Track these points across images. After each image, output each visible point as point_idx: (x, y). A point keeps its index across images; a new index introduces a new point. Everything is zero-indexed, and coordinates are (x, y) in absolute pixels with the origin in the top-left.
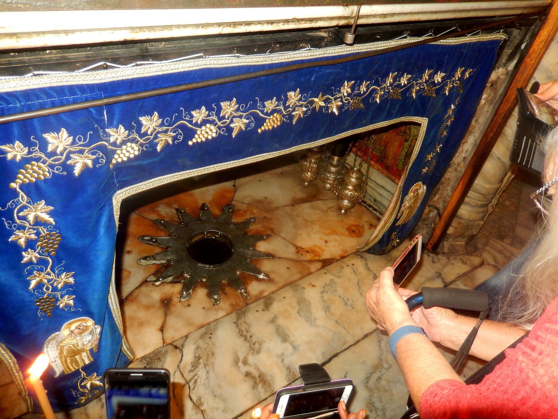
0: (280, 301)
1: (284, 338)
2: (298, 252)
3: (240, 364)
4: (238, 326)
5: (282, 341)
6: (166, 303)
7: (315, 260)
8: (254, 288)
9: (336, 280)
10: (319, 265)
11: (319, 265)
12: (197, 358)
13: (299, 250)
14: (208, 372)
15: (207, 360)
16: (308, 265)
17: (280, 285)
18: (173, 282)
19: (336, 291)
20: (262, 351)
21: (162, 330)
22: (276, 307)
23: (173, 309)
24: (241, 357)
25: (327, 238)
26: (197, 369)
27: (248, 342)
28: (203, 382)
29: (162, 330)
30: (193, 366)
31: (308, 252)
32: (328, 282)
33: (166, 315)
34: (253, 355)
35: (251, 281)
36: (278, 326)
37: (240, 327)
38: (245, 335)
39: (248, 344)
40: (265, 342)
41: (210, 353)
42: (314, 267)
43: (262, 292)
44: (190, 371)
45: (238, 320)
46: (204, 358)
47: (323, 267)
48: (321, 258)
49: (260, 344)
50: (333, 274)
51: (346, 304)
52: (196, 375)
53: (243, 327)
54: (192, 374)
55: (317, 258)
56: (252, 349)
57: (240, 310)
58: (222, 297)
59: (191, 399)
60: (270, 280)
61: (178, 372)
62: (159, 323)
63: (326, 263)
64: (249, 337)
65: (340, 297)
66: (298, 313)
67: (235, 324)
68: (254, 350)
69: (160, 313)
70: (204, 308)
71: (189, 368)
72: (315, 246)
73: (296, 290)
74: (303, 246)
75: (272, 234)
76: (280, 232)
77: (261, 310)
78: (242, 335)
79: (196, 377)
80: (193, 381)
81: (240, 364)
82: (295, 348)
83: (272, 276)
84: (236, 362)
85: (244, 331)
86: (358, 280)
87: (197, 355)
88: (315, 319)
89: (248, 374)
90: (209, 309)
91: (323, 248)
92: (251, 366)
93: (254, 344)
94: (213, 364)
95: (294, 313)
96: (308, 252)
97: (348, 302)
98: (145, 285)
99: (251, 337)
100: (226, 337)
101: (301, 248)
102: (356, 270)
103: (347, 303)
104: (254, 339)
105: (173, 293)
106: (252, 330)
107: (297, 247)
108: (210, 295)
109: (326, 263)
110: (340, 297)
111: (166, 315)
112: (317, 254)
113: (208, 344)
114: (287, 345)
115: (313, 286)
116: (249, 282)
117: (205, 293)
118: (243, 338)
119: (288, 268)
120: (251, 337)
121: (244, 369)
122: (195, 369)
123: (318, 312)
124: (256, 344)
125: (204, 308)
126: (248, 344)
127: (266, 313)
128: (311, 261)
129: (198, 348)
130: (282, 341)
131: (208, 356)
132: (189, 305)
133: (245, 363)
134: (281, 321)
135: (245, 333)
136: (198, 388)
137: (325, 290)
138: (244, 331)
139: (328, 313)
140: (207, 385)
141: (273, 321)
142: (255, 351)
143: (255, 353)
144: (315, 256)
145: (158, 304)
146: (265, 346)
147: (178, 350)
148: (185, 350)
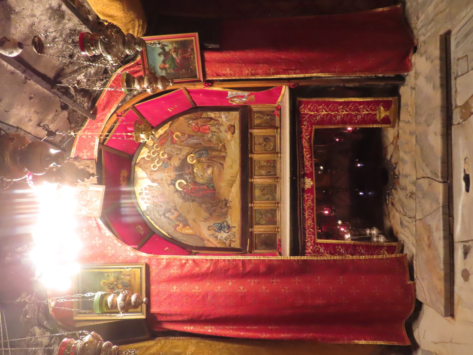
1: (406, 176)
13: (392, 143)
18: (389, 197)
23: (394, 203)
33: (394, 207)
38: (402, 189)
51: (407, 143)
62: (396, 211)
63: (398, 136)
82: (410, 175)
84: (407, 198)
89: (410, 197)
114: (409, 177)
121: (408, 197)
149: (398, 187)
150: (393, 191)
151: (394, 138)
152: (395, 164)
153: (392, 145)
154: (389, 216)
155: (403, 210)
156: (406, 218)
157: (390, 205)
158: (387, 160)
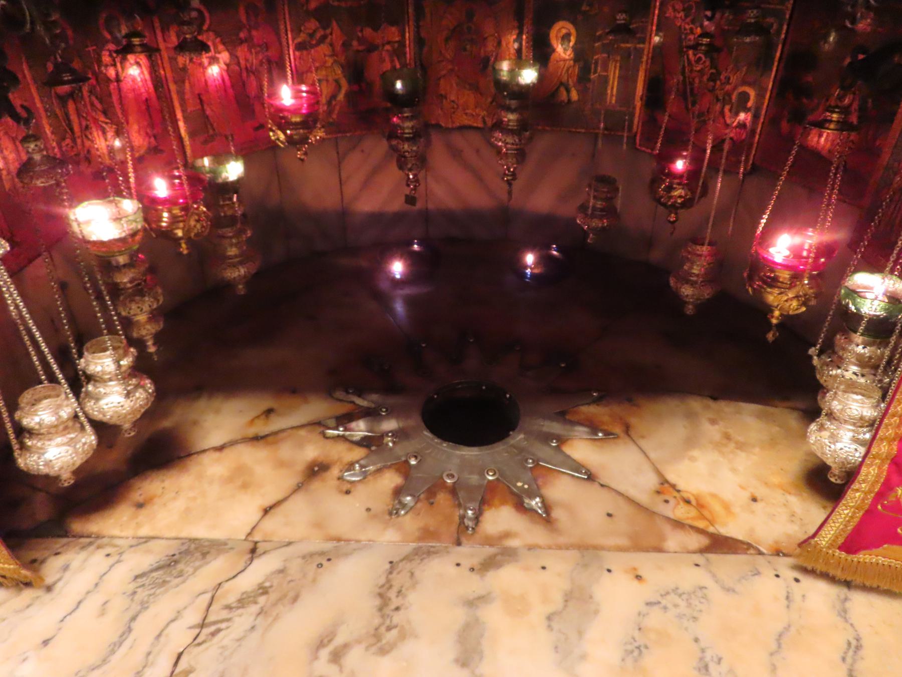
0: (526, 569)
2: (658, 492)
3: (324, 653)
4: (391, 573)
5: (457, 661)
6: (316, 470)
7: (692, 527)
8: (500, 519)
9: (715, 592)
10: (696, 541)
11: (696, 541)
12: (263, 590)
13: (665, 487)
14: (253, 628)
15: (275, 604)
16: (667, 529)
17: (562, 540)
19: (695, 619)
20: (394, 653)
21: (266, 511)
22: (508, 577)
23: (316, 485)
24: (339, 640)
25: (760, 492)
26: (240, 611)
27: (383, 616)
28: (226, 642)
29: (266, 511)
30: (240, 601)
31: (688, 502)
32: (686, 586)
33: (298, 488)
34: (367, 649)
35: (504, 502)
36: (477, 620)
37: (394, 575)
38: (386, 598)
39: (377, 621)
40: (416, 637)
41: (291, 594)
42: (674, 540)
43: (507, 535)
44: (229, 607)
45: (402, 560)
46: (273, 596)
47: (703, 551)
48: (711, 529)
49: (403, 636)
50: (714, 576)
52: (228, 620)
53: (398, 580)
54: (225, 614)
55: (701, 524)
56: (376, 635)
57: (426, 545)
58: (419, 505)
59: (176, 664)
60: (546, 518)
61: (208, 596)
63: (720, 545)
64: (393, 607)
65: (696, 640)
66: (549, 618)
67: (388, 566)
68: (379, 640)
69: (289, 480)
70: (368, 510)
71: (232, 599)
72: (714, 496)
73: (586, 566)
74: (681, 485)
75: (622, 435)
76: (643, 437)
77: (469, 566)
78: (381, 595)
79: (223, 625)
80: (213, 628)
81: (324, 653)
83: (556, 513)
84: (321, 644)
85: (395, 590)
86: (788, 628)
87: (267, 584)
88: (583, 657)
90: (375, 517)
91: (736, 509)
92: (341, 671)
93: (389, 629)
94: (276, 619)
95: (539, 611)
96: (688, 502)
97: (712, 667)
98: (309, 428)
99: (397, 609)
100: (350, 583)
101: (673, 486)
102: (797, 597)
103: (706, 667)
104: (397, 618)
105: (340, 460)
106: (412, 597)
107: (664, 482)
108: (398, 492)
109: (720, 545)
110: (696, 640)
111: (298, 488)
112: (706, 513)
113: (305, 575)
115: (638, 577)
116: (496, 501)
117: (393, 485)
118: (378, 602)
119: (609, 515)
120: (397, 609)
122: (238, 608)
123: (603, 645)
124: (394, 632)
125: (368, 510)
126: (377, 621)
127: (475, 577)
128: (678, 524)
129: (281, 571)
130: (457, 661)
131: (280, 600)
132: (348, 492)
133: (336, 657)
134: (493, 615)
135: (392, 594)
136: (207, 649)
137: (664, 602)
138: (395, 590)
139: (629, 661)
140: (227, 653)
141: (473, 603)
142: (379, 645)
143: (374, 649)
144: (703, 517)
145: (300, 467)
146: (408, 648)
147: (250, 556)
148: (256, 562)
149: (410, 522)
150: (391, 480)
151: (698, 504)
152: (547, 507)
153: (650, 481)
154: (256, 439)
155: (243, 602)
156: (179, 636)
157: (311, 450)
158: (562, 440)
